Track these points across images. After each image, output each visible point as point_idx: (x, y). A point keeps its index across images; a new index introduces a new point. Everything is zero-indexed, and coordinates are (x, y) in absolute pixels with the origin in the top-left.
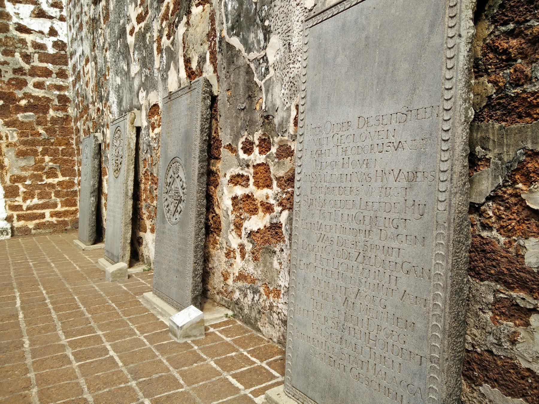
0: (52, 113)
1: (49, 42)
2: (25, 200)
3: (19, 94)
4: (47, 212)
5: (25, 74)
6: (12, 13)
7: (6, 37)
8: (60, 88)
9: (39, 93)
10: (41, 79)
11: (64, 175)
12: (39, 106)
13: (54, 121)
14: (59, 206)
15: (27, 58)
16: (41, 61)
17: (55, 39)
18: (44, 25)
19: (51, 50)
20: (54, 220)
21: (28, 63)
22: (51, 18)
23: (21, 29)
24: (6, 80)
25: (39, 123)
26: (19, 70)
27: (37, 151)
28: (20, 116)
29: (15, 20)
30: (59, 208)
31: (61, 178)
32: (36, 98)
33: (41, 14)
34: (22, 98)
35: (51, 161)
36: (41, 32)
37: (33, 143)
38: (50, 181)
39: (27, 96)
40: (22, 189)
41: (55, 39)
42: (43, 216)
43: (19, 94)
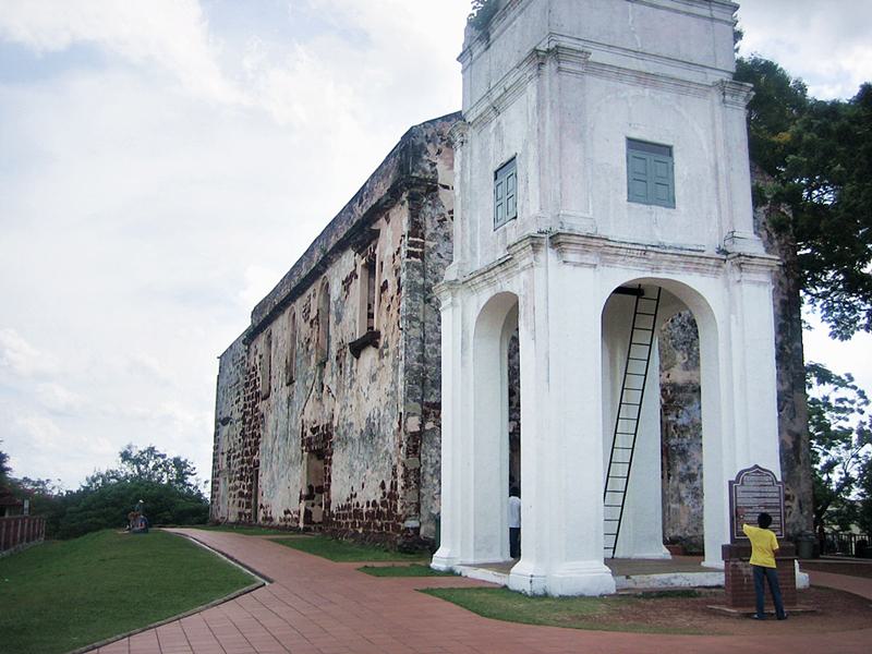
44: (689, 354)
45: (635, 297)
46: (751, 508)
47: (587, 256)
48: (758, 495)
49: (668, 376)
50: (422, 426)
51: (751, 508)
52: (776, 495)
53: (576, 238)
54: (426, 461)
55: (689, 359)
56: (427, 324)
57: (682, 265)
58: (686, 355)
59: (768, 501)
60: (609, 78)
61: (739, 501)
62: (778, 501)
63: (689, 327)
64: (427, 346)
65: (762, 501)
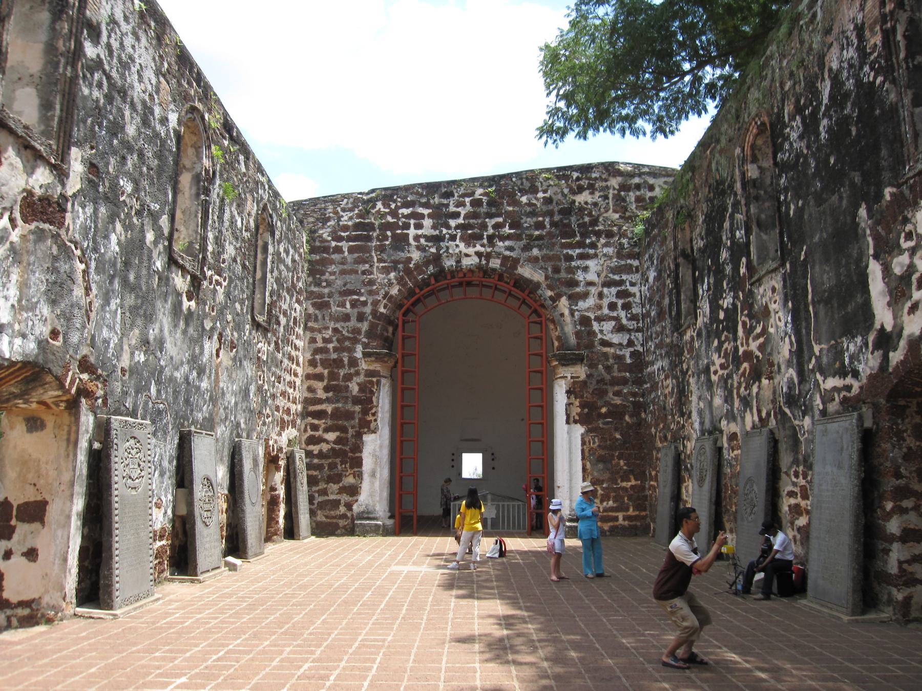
0: (627, 418)
1: (627, 353)
2: (602, 502)
4: (620, 515)
5: (606, 384)
6: (597, 331)
8: (634, 395)
9: (618, 401)
11: (636, 479)
12: (616, 413)
14: (631, 509)
15: (608, 369)
16: (620, 371)
19: (629, 361)
20: (626, 523)
21: (609, 373)
22: (629, 331)
23: (605, 343)
25: (616, 430)
26: (601, 381)
27: (613, 455)
29: (599, 336)
30: (631, 512)
31: (633, 482)
32: (616, 406)
33: (620, 328)
34: (603, 406)
35: (625, 464)
36: (620, 344)
37: (611, 448)
38: (624, 484)
39: (607, 404)
40: (600, 492)
41: (632, 350)
42: (616, 519)
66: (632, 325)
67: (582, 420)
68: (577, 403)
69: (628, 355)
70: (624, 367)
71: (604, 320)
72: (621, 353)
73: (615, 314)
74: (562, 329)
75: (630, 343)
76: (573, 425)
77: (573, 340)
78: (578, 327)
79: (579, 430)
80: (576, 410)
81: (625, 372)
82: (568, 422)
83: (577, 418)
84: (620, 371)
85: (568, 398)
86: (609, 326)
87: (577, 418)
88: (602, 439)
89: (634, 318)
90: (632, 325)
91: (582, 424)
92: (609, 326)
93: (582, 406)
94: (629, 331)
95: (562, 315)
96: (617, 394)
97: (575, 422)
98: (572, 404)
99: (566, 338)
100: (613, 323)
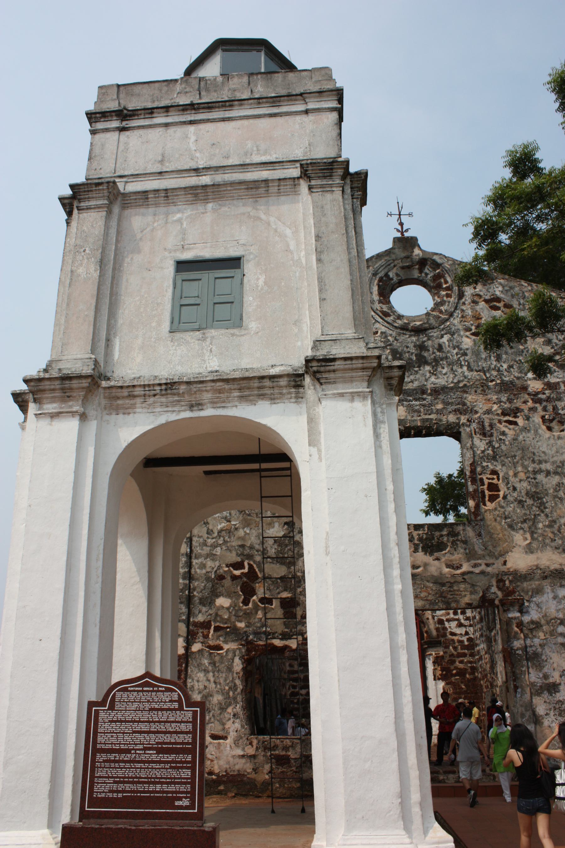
0: (468, 676)
1: (465, 639)
3: (452, 667)
7: (446, 639)
8: (471, 662)
9: (461, 666)
10: (461, 659)
12: (462, 673)
13: (469, 680)
15: (455, 648)
16: (462, 649)
17: (467, 637)
18: (462, 630)
19: (466, 643)
21: (456, 651)
22: (465, 626)
23: (453, 634)
24: (446, 661)
25: (462, 683)
26: (452, 655)
28: (453, 679)
29: (449, 630)
32: (460, 669)
33: (460, 625)
34: (453, 670)
36: (461, 634)
39: (456, 668)
41: (467, 637)
43: (452, 667)
44: (532, 533)
45: (262, 453)
46: (128, 751)
47: (71, 403)
48: (144, 727)
49: (505, 563)
50: (187, 648)
51: (128, 751)
52: (183, 727)
53: (47, 383)
54: (193, 687)
55: (533, 538)
56: (195, 539)
57: (236, 394)
58: (528, 536)
59: (167, 738)
60: (157, 205)
61: (99, 739)
62: (188, 738)
63: (529, 502)
64: (194, 561)
65: (153, 739)
66: (467, 623)
67: (443, 678)
68: (439, 669)
69: (465, 640)
70: (464, 647)
71: (451, 621)
72: (462, 639)
73: (457, 617)
74: (428, 627)
75: (467, 633)
76: (437, 681)
77: (434, 633)
78: (437, 625)
79: (441, 684)
80: (439, 673)
81: (465, 649)
82: (435, 679)
83: (440, 677)
84: (462, 649)
85: (434, 666)
86: (454, 624)
87: (440, 677)
88: (454, 689)
89: (468, 619)
90: (467, 623)
91: (443, 680)
92: (454, 624)
93: (442, 670)
94: (465, 626)
95: (428, 619)
96: (461, 662)
97: (439, 679)
98: (436, 669)
99: (431, 632)
100: (456, 622)
